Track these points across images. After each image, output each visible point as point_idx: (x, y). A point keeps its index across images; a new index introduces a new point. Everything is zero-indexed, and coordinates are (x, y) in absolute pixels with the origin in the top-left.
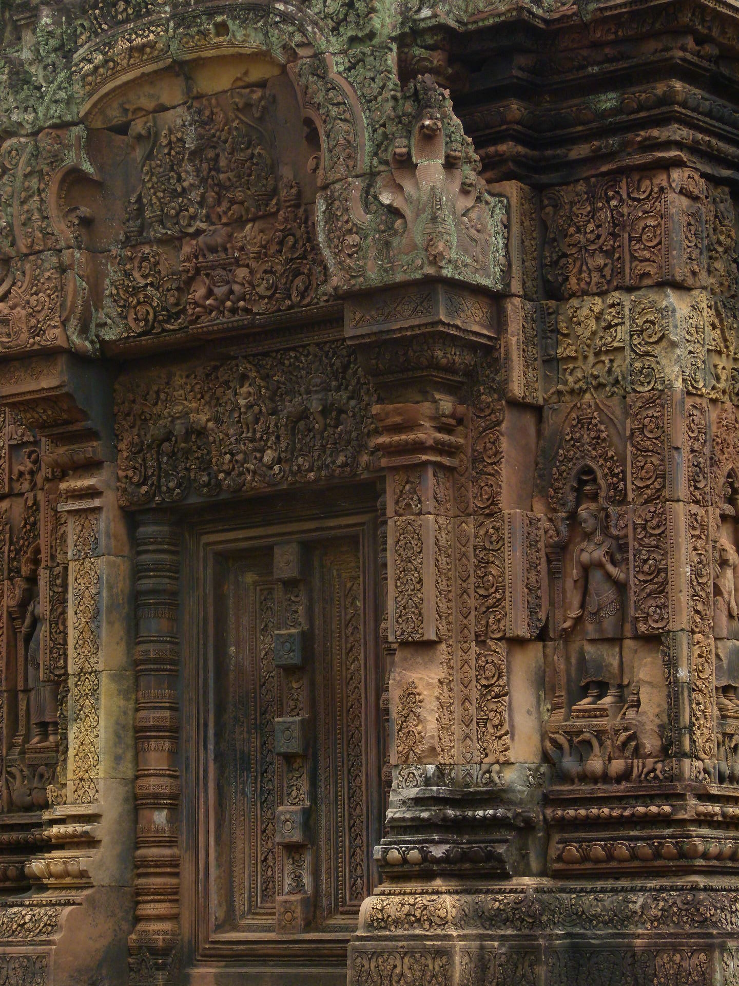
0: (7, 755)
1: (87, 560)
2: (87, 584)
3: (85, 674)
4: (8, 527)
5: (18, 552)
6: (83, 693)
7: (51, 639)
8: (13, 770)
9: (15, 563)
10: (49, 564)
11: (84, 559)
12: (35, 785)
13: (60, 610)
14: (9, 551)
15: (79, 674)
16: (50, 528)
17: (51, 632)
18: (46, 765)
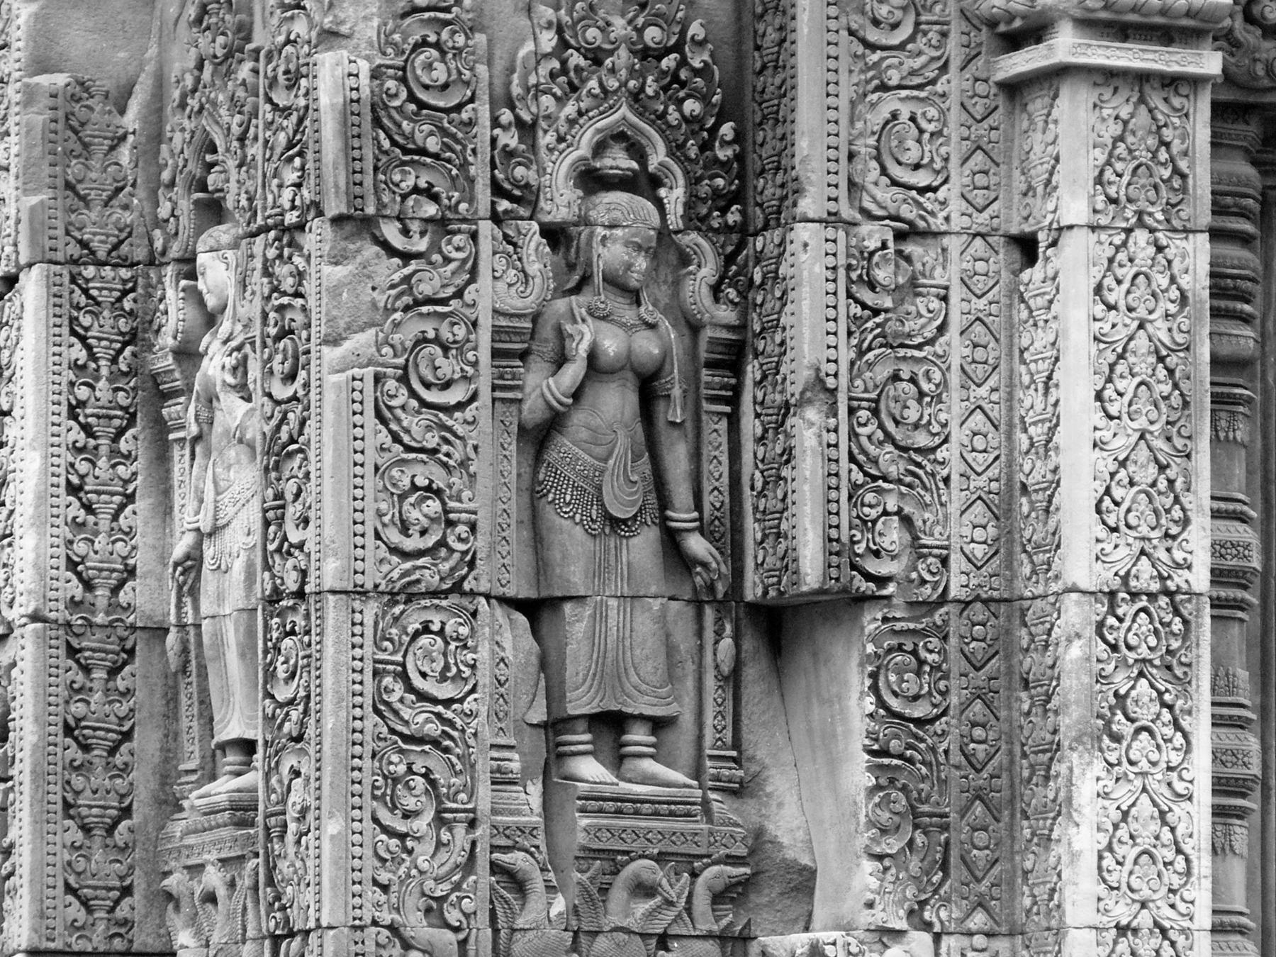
0: (494, 812)
1: (1141, 236)
2: (1142, 312)
3: (1134, 595)
4: (480, 39)
5: (527, 129)
6: (1131, 656)
7: (852, 459)
8: (517, 859)
9: (520, 172)
10: (847, 212)
11: (1129, 231)
12: (614, 919)
13: (882, 372)
14: (495, 123)
15: (1112, 594)
16: (846, 92)
17: (853, 435)
18: (661, 858)
